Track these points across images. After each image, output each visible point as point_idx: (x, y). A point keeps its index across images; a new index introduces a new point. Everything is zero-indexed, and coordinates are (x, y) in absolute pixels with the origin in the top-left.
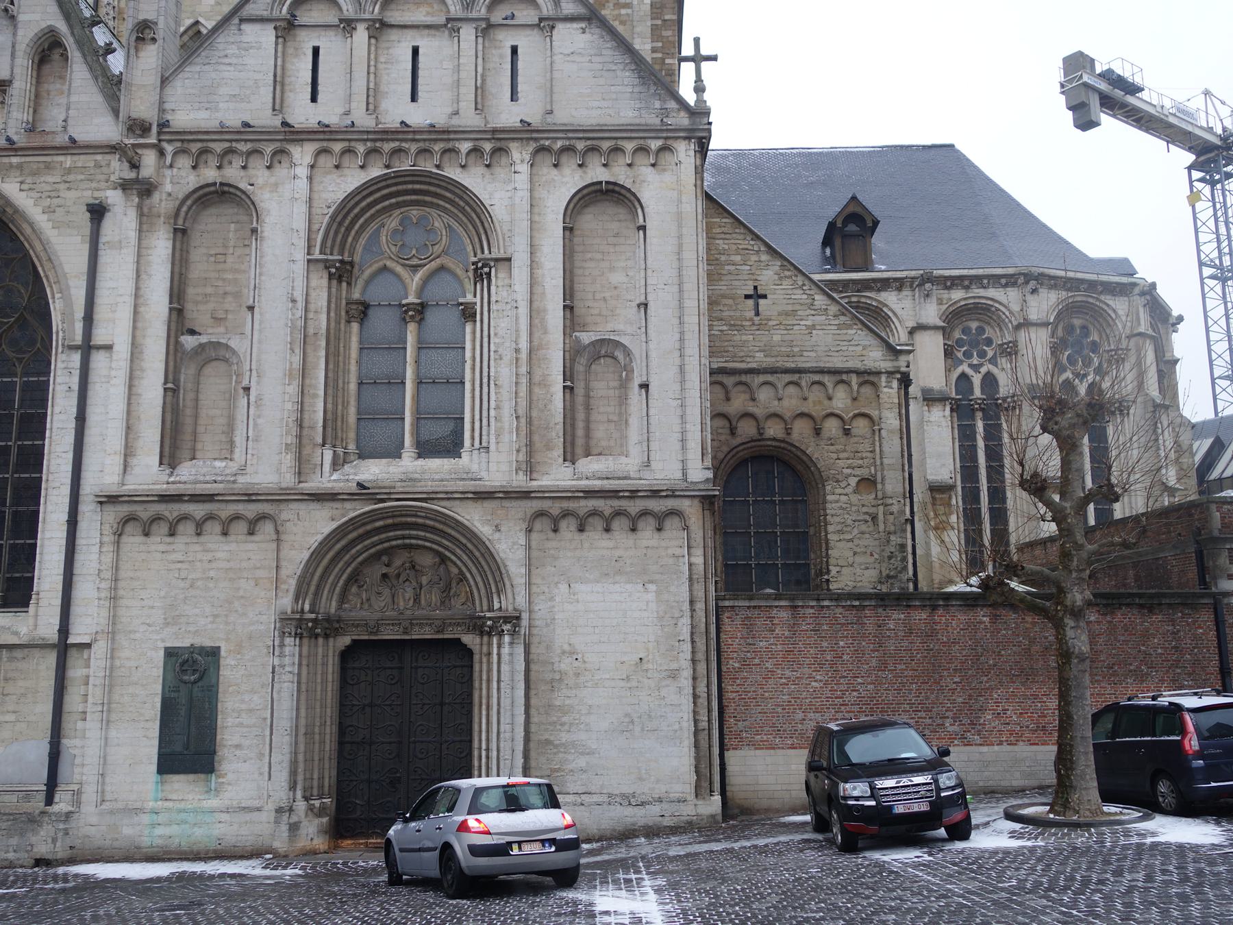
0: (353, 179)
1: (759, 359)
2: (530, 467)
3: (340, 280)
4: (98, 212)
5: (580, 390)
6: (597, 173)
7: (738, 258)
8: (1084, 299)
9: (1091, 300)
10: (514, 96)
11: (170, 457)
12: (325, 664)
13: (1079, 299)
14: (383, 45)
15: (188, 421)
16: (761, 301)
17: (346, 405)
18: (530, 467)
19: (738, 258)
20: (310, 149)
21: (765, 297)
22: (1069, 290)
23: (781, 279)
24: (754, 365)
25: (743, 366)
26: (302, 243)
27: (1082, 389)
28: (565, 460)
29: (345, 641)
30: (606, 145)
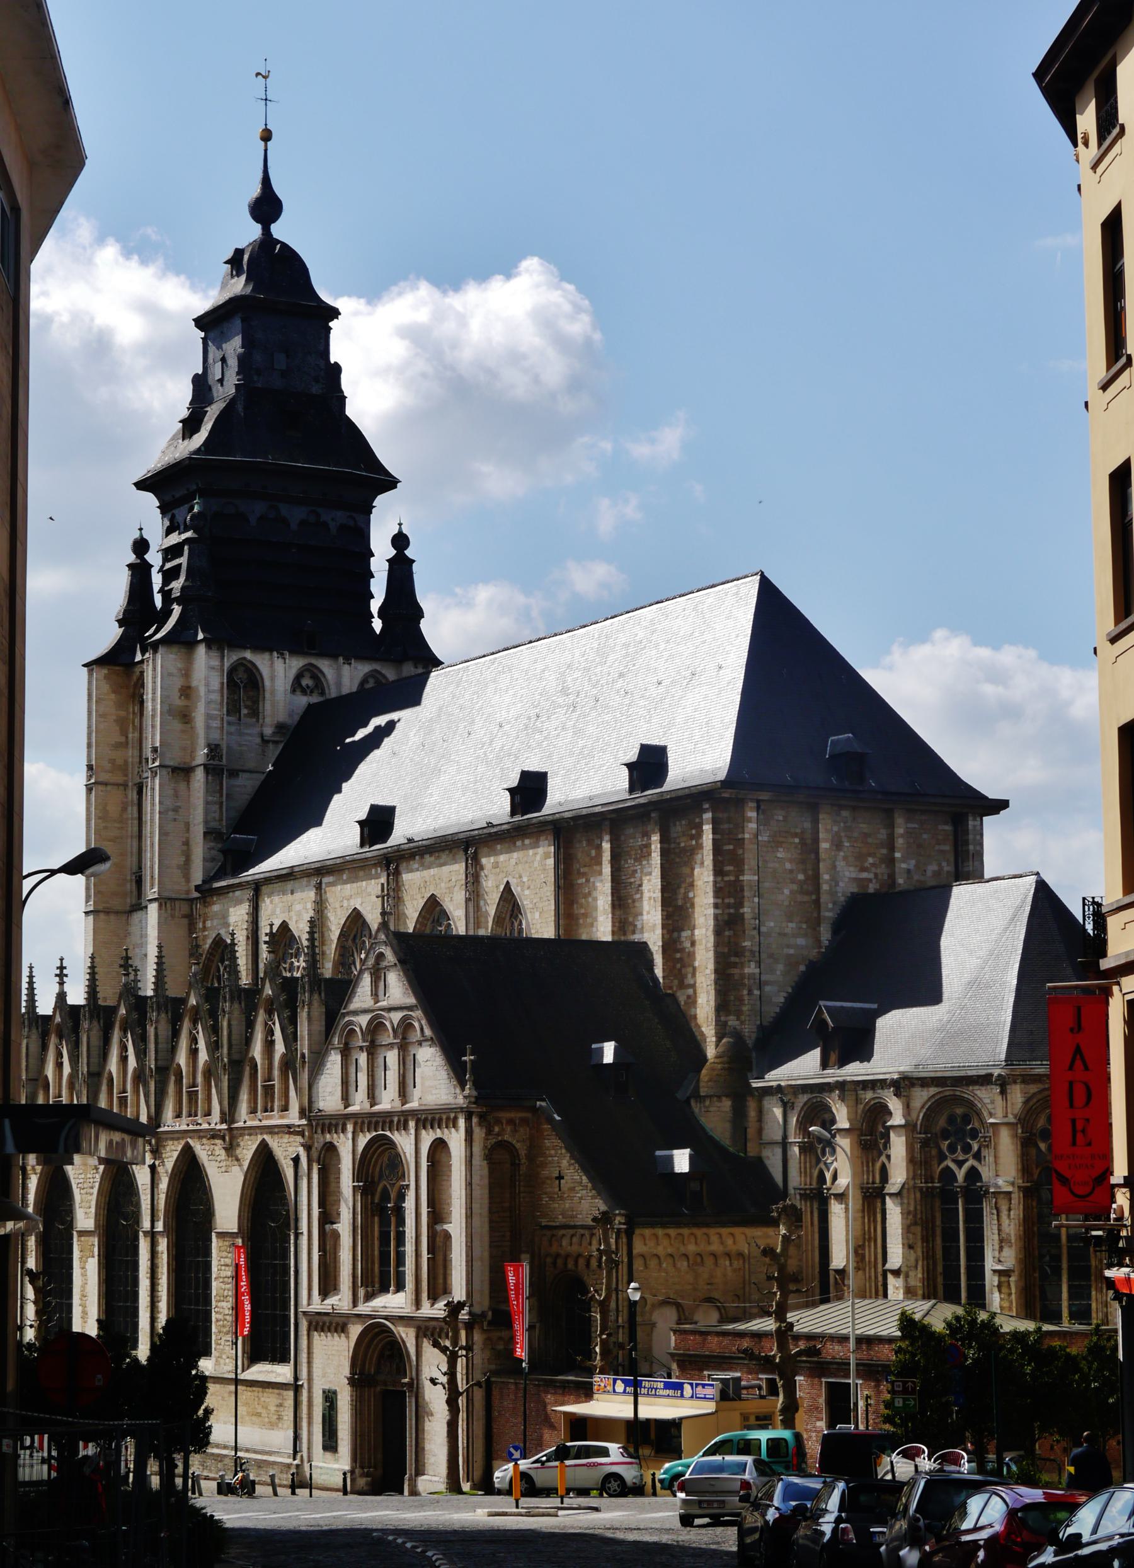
0: (369, 1136)
1: (561, 1220)
2: (418, 1304)
3: (367, 1195)
4: (296, 1160)
5: (440, 1258)
6: (439, 1133)
7: (553, 1152)
8: (952, 1093)
9: (958, 1093)
10: (415, 1087)
11: (325, 1293)
12: (369, 1400)
13: (947, 1093)
14: (376, 1056)
15: (332, 1270)
16: (562, 1181)
17: (373, 1263)
18: (418, 1304)
19: (553, 1152)
20: (352, 1121)
21: (563, 1178)
22: (937, 1086)
23: (570, 1165)
24: (558, 1224)
25: (554, 1224)
26: (351, 1176)
27: (961, 1174)
28: (429, 1299)
29: (378, 1389)
30: (437, 1116)
